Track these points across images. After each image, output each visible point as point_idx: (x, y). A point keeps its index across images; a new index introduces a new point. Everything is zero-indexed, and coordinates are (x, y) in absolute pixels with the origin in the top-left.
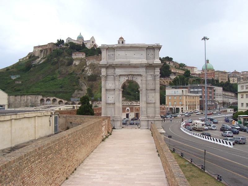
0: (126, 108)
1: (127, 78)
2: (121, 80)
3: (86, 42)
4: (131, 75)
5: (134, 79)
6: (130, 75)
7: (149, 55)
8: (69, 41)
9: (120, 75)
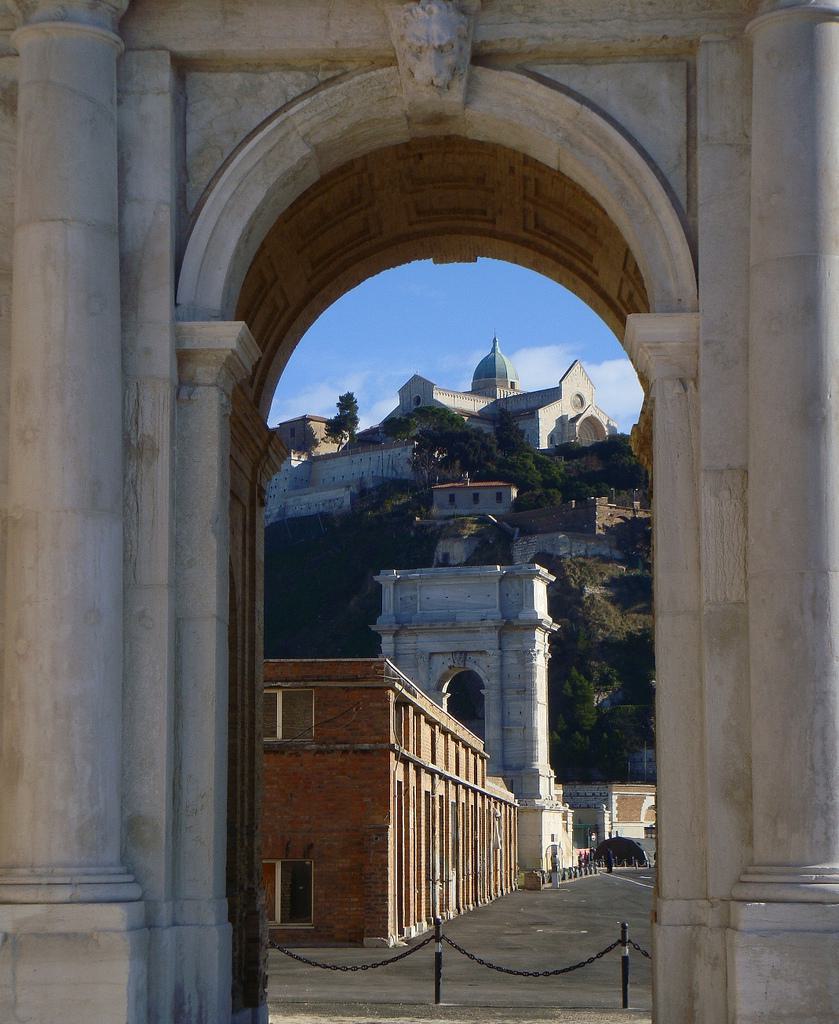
0: (643, 798)
1: (450, 663)
2: (434, 668)
3: (532, 404)
4: (461, 652)
5: (470, 666)
6: (456, 652)
7: (510, 596)
8: (418, 400)
9: (432, 654)
